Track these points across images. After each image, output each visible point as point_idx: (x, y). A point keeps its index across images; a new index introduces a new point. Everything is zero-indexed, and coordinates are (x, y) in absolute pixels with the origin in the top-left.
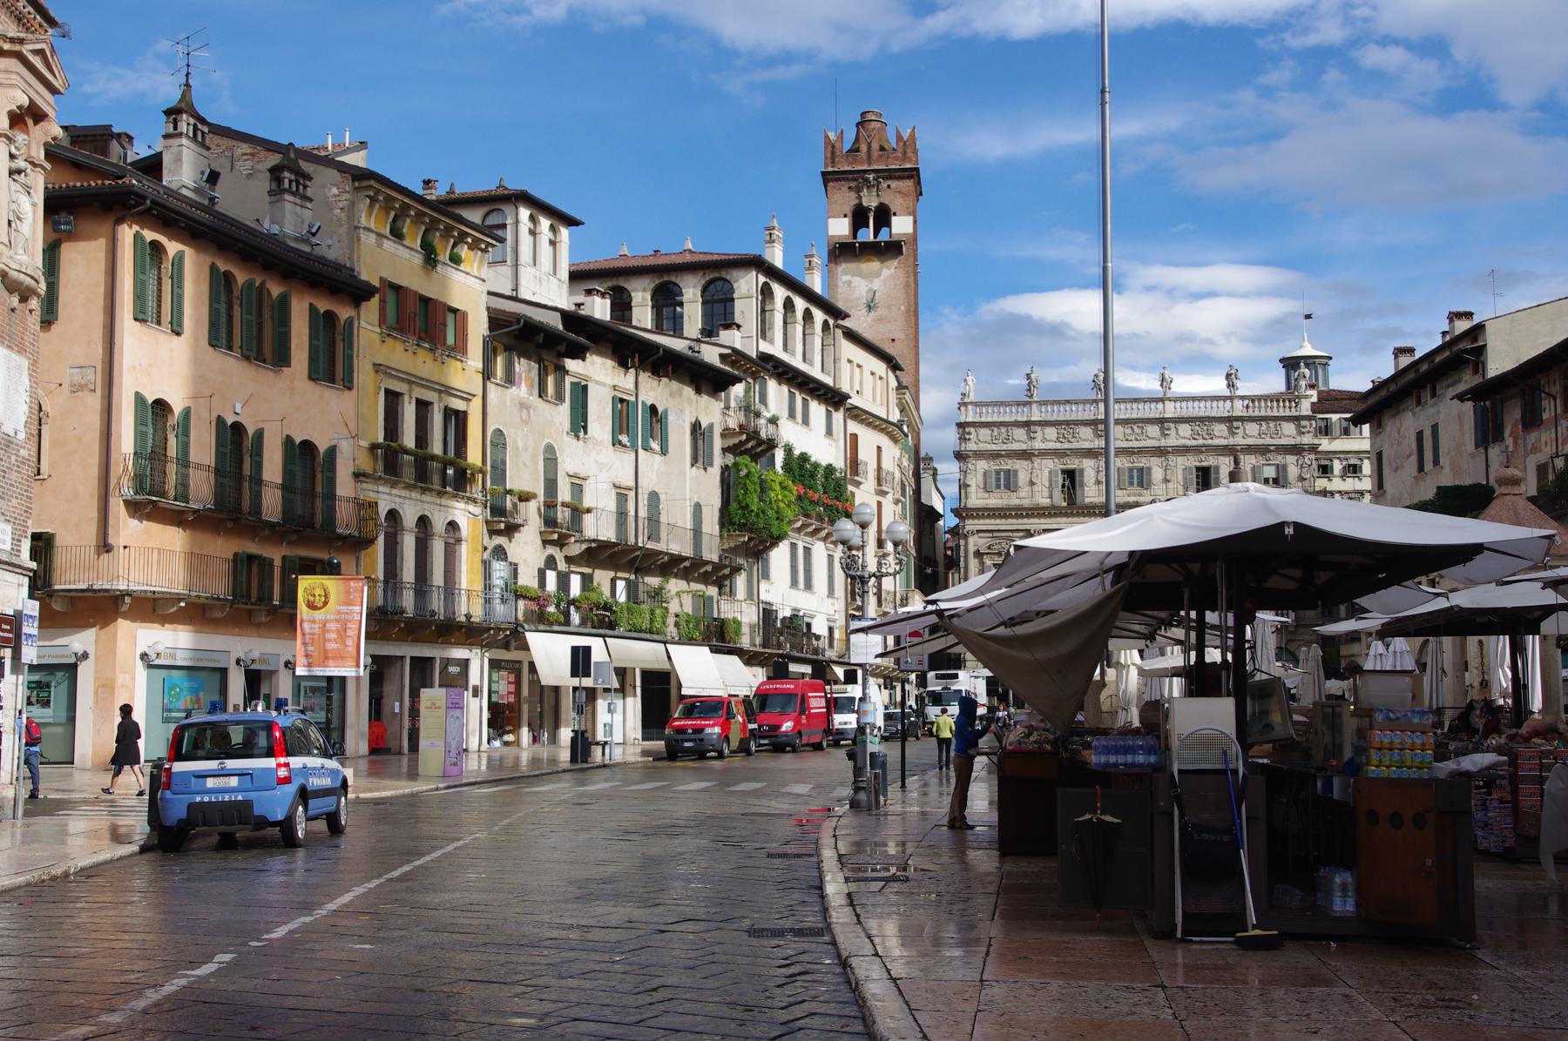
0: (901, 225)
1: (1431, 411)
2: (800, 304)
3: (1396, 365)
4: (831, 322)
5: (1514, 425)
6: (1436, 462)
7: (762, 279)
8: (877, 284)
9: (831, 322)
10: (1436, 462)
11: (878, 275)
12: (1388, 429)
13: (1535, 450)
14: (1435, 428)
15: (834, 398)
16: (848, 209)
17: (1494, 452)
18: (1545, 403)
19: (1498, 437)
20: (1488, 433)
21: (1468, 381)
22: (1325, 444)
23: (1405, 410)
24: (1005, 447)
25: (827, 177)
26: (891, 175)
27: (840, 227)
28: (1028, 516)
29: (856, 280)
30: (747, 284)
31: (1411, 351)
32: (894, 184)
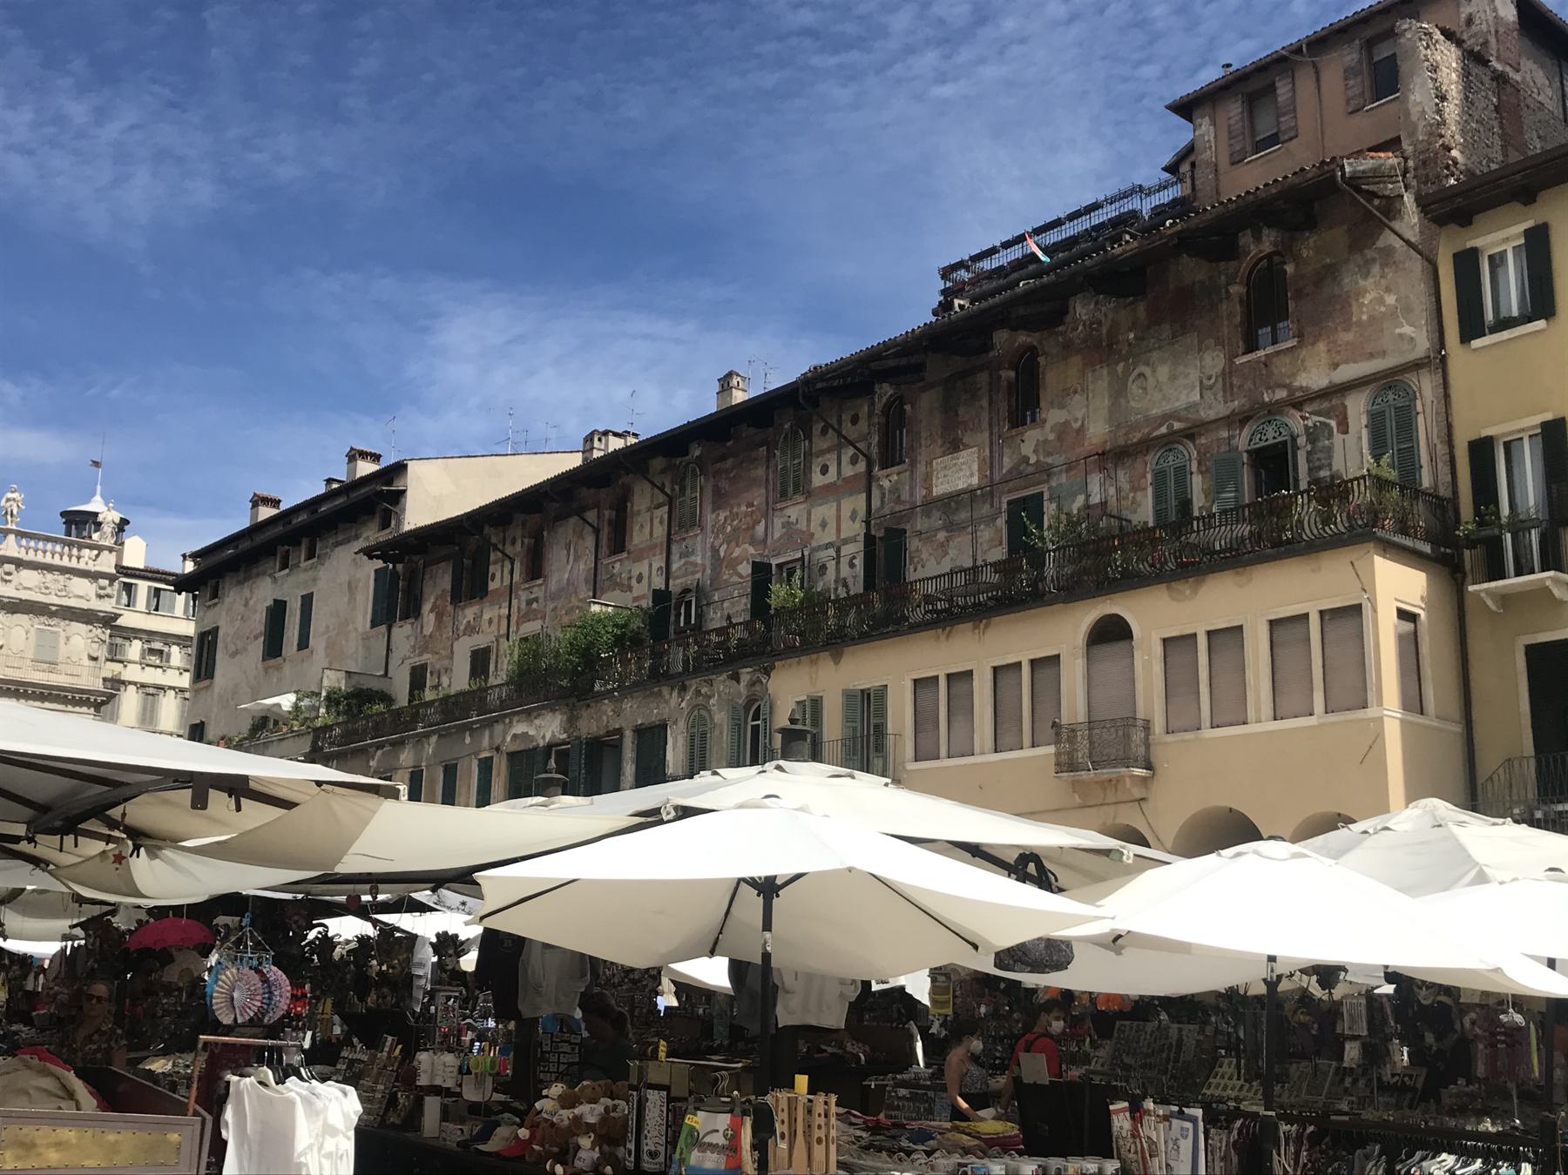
3: (255, 515)
5: (441, 596)
6: (303, 643)
10: (303, 643)
12: (227, 600)
13: (471, 629)
14: (307, 601)
17: (403, 633)
19: (412, 611)
20: (396, 602)
21: (372, 535)
22: (128, 619)
23: (264, 573)
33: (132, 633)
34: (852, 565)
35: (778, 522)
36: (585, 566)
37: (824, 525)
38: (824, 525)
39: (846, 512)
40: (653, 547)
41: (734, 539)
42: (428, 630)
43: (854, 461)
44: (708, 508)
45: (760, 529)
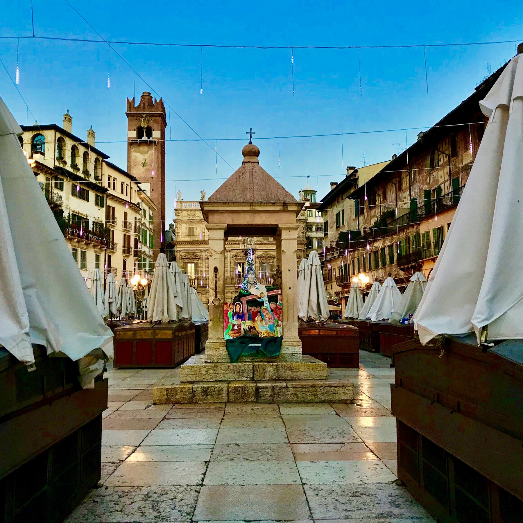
0: (156, 134)
1: (341, 205)
2: (82, 149)
4: (101, 159)
6: (343, 224)
7: (58, 135)
8: (146, 156)
9: (101, 159)
10: (343, 224)
11: (147, 152)
14: (343, 210)
15: (101, 191)
16: (135, 128)
17: (361, 218)
18: (377, 198)
22: (310, 220)
24: (193, 218)
25: (128, 115)
26: (152, 115)
27: (133, 134)
28: (200, 244)
29: (138, 154)
30: (50, 136)
31: (337, 183)
32: (153, 118)
33: (312, 224)
34: (448, 189)
35: (432, 177)
36: (394, 195)
37: (441, 177)
38: (441, 177)
39: (445, 173)
40: (407, 188)
41: (423, 184)
42: (366, 217)
43: (446, 157)
44: (417, 174)
45: (428, 180)
